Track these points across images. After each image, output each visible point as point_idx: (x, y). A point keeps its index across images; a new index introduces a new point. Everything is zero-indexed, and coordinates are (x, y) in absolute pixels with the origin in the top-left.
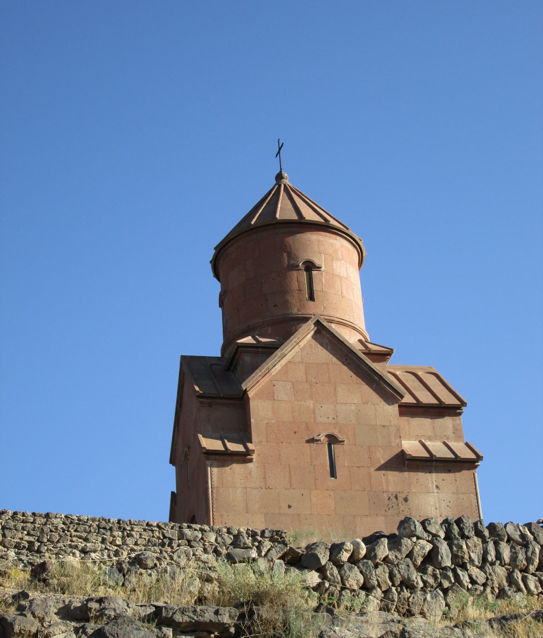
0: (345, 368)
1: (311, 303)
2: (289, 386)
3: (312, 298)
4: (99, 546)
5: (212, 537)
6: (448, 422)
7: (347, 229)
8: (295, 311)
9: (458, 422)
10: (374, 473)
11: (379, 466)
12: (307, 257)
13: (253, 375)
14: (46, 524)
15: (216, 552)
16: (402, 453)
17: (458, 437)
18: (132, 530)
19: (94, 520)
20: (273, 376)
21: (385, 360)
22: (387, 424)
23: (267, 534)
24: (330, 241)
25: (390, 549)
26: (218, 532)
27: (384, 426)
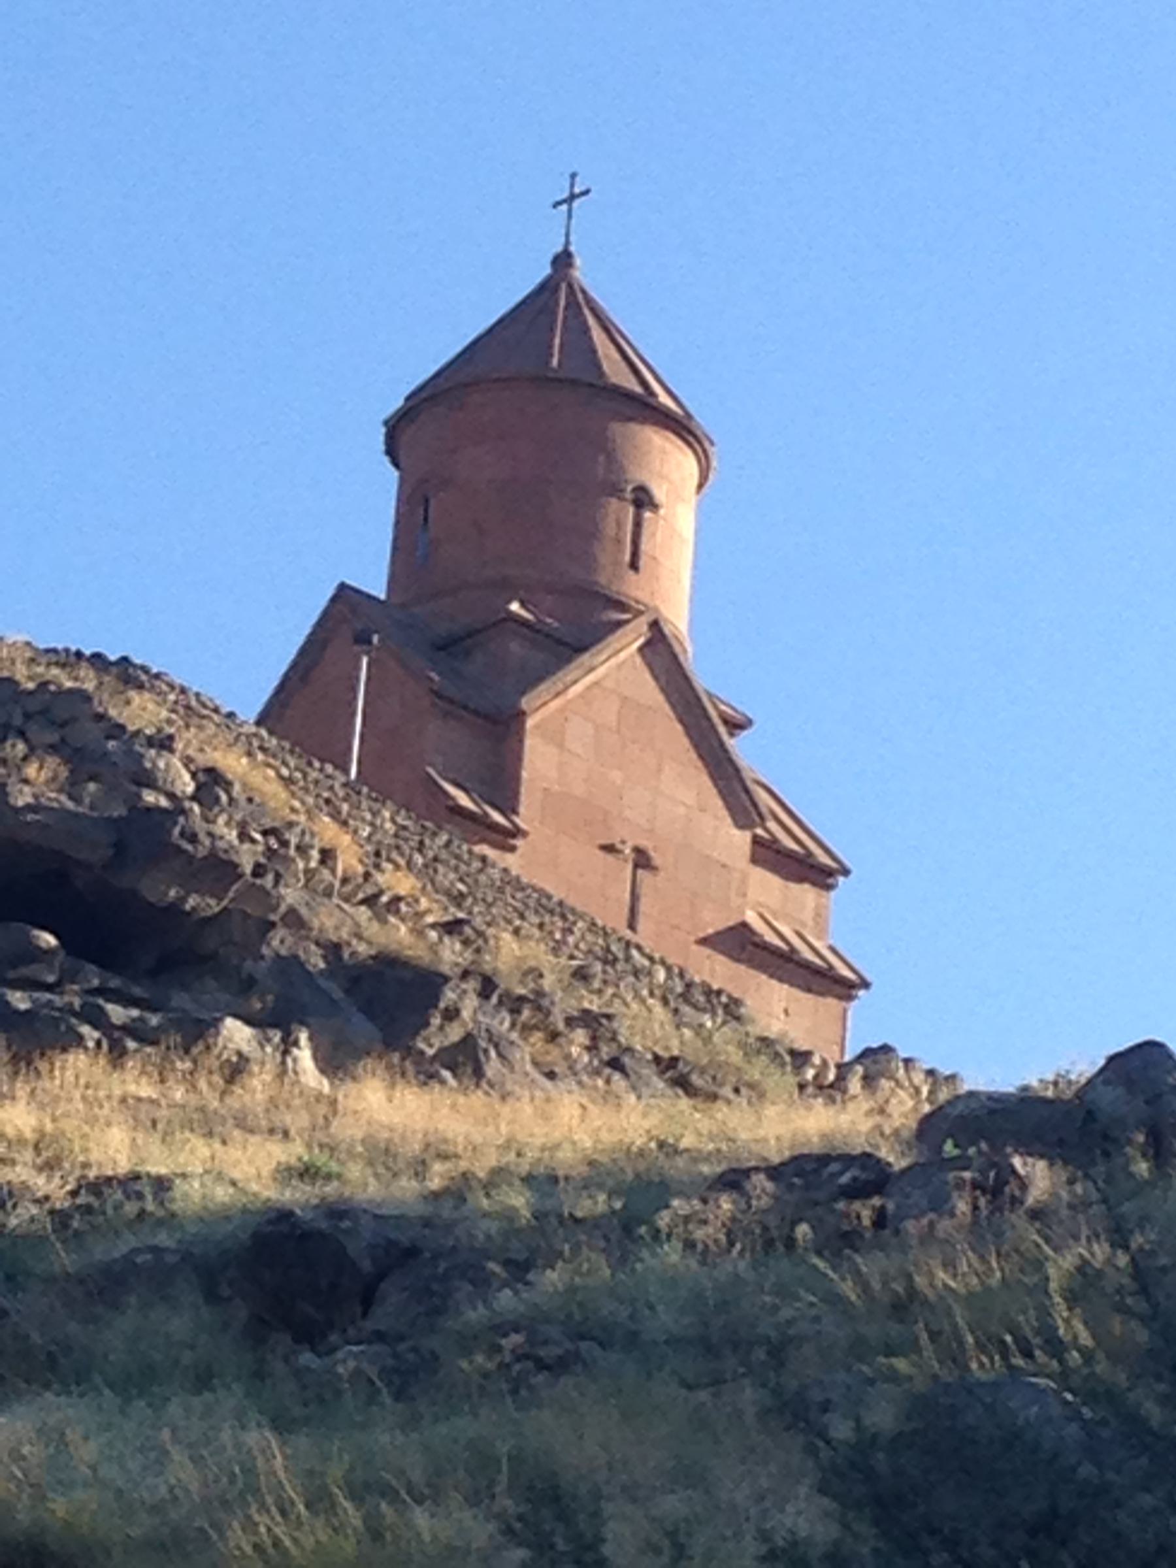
0: (679, 727)
1: (631, 573)
2: (590, 729)
3: (634, 566)
4: (536, 933)
5: (661, 975)
6: (806, 894)
7: (712, 443)
8: (603, 580)
9: (824, 900)
10: (695, 947)
11: (701, 935)
12: (643, 478)
13: (542, 687)
14: (481, 871)
15: (665, 1001)
16: (744, 925)
17: (821, 933)
18: (574, 923)
19: (535, 889)
20: (569, 701)
21: (732, 735)
22: (729, 863)
23: (724, 999)
24: (680, 457)
25: (863, 1087)
26: (669, 969)
27: (724, 866)
